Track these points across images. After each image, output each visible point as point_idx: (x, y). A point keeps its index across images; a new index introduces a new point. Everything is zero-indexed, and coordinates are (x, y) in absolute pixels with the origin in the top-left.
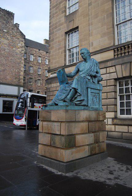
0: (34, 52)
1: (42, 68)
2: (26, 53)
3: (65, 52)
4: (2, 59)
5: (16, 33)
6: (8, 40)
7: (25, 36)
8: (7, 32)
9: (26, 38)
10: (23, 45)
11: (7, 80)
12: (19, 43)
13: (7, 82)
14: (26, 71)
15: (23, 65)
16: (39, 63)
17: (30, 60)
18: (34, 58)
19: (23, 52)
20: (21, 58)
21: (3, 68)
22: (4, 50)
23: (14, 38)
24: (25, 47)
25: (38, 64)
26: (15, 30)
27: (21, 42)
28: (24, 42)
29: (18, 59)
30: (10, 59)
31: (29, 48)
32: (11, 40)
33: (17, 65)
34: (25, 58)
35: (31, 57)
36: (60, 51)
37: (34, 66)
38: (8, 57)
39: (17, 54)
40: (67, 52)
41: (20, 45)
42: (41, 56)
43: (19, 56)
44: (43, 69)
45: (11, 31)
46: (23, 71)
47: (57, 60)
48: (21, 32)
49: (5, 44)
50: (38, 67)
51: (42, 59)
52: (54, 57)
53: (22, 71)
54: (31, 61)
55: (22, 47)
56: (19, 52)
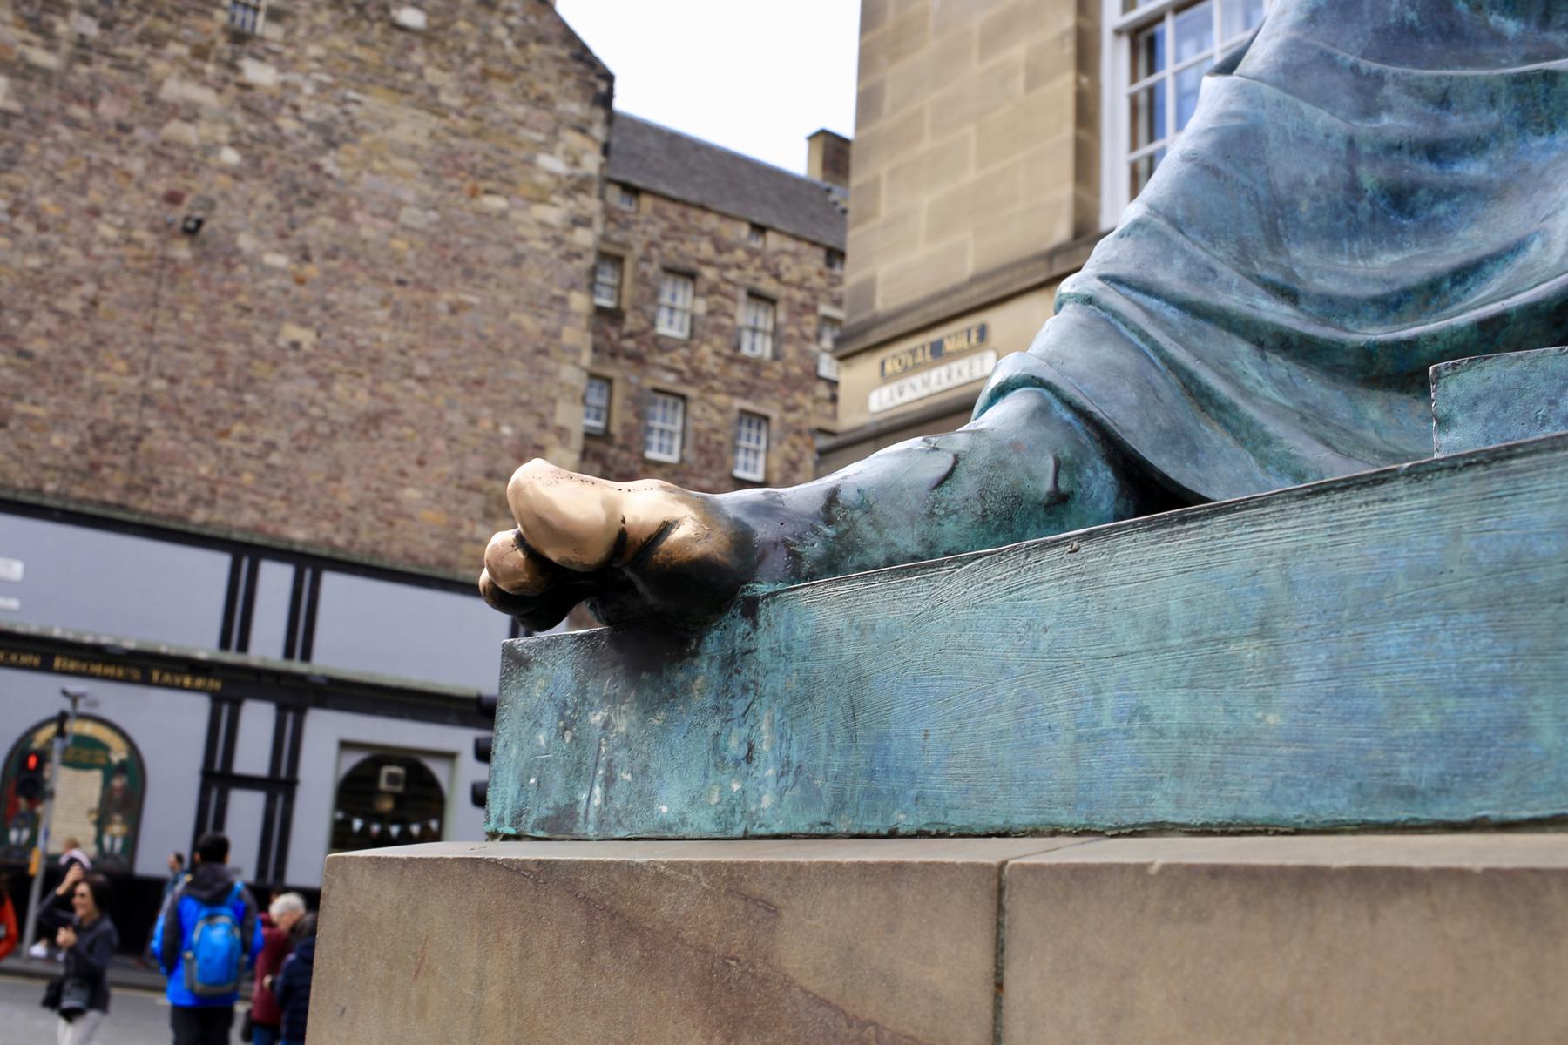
0: (706, 249)
1: (775, 414)
2: (611, 258)
3: (1086, 55)
4: (361, 299)
5: (520, 44)
6: (438, 111)
7: (609, 78)
8: (427, 37)
9: (619, 104)
10: (592, 163)
11: (400, 522)
12: (547, 147)
13: (393, 553)
14: (605, 436)
15: (571, 376)
16: (745, 361)
17: (653, 324)
18: (701, 306)
19: (584, 238)
20: (563, 300)
21: (363, 400)
22: (390, 211)
23: (499, 91)
24: (614, 194)
25: (738, 372)
26: (509, 12)
27: (573, 139)
28: (598, 131)
29: (533, 306)
30: (442, 307)
31: (647, 202)
32: (461, 114)
33: (519, 373)
34: (600, 311)
35: (665, 299)
36: (1018, 52)
37: (691, 392)
38: (419, 283)
39: (517, 261)
40: (1115, 59)
41: (551, 163)
42: (768, 285)
43: (536, 280)
44: (787, 428)
45: (472, 19)
46: (577, 442)
47: (971, 175)
48: (570, 37)
49: (399, 152)
50: (739, 403)
51: (782, 317)
52: (927, 144)
53: (562, 433)
54: (662, 345)
55: (579, 186)
56: (536, 232)
